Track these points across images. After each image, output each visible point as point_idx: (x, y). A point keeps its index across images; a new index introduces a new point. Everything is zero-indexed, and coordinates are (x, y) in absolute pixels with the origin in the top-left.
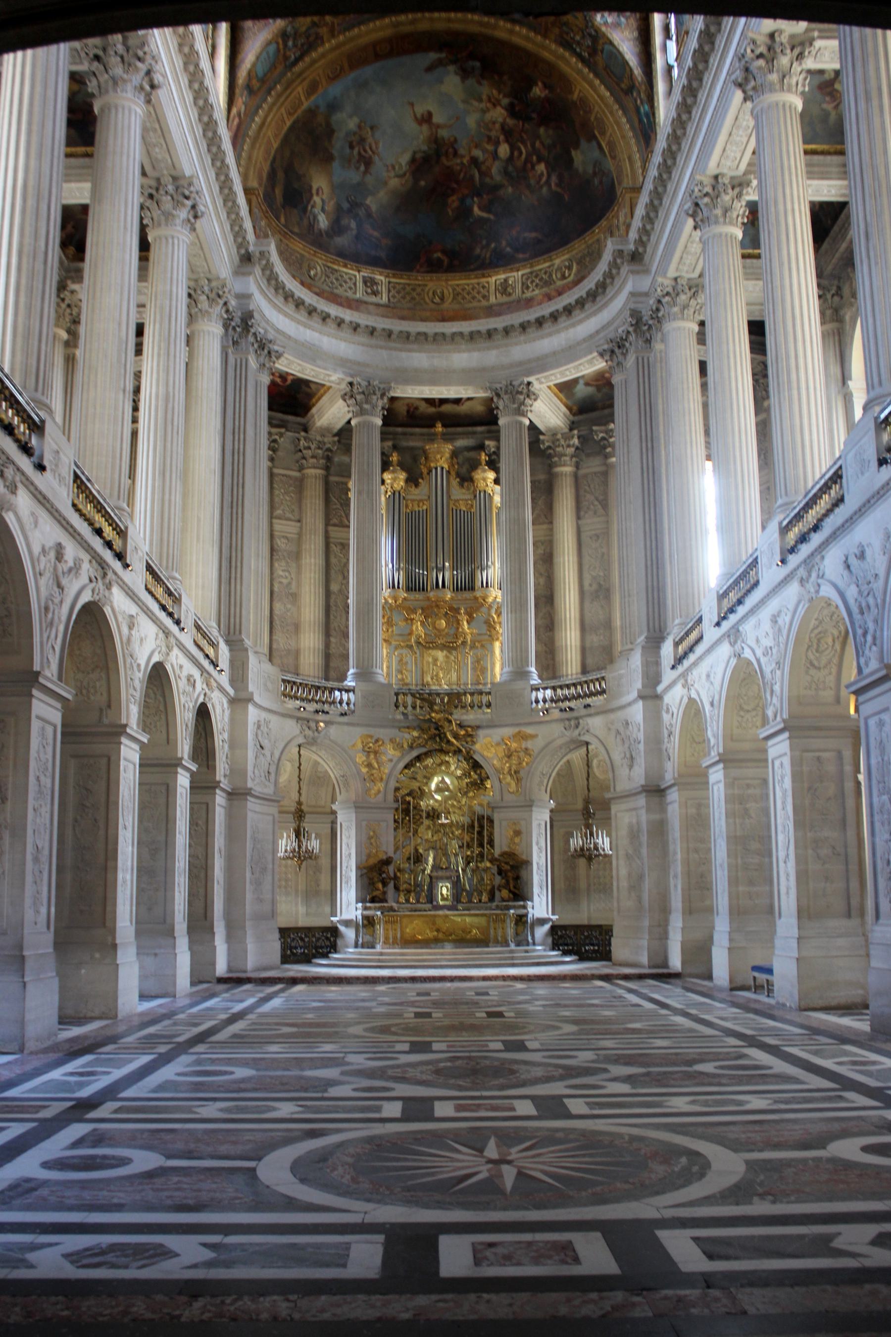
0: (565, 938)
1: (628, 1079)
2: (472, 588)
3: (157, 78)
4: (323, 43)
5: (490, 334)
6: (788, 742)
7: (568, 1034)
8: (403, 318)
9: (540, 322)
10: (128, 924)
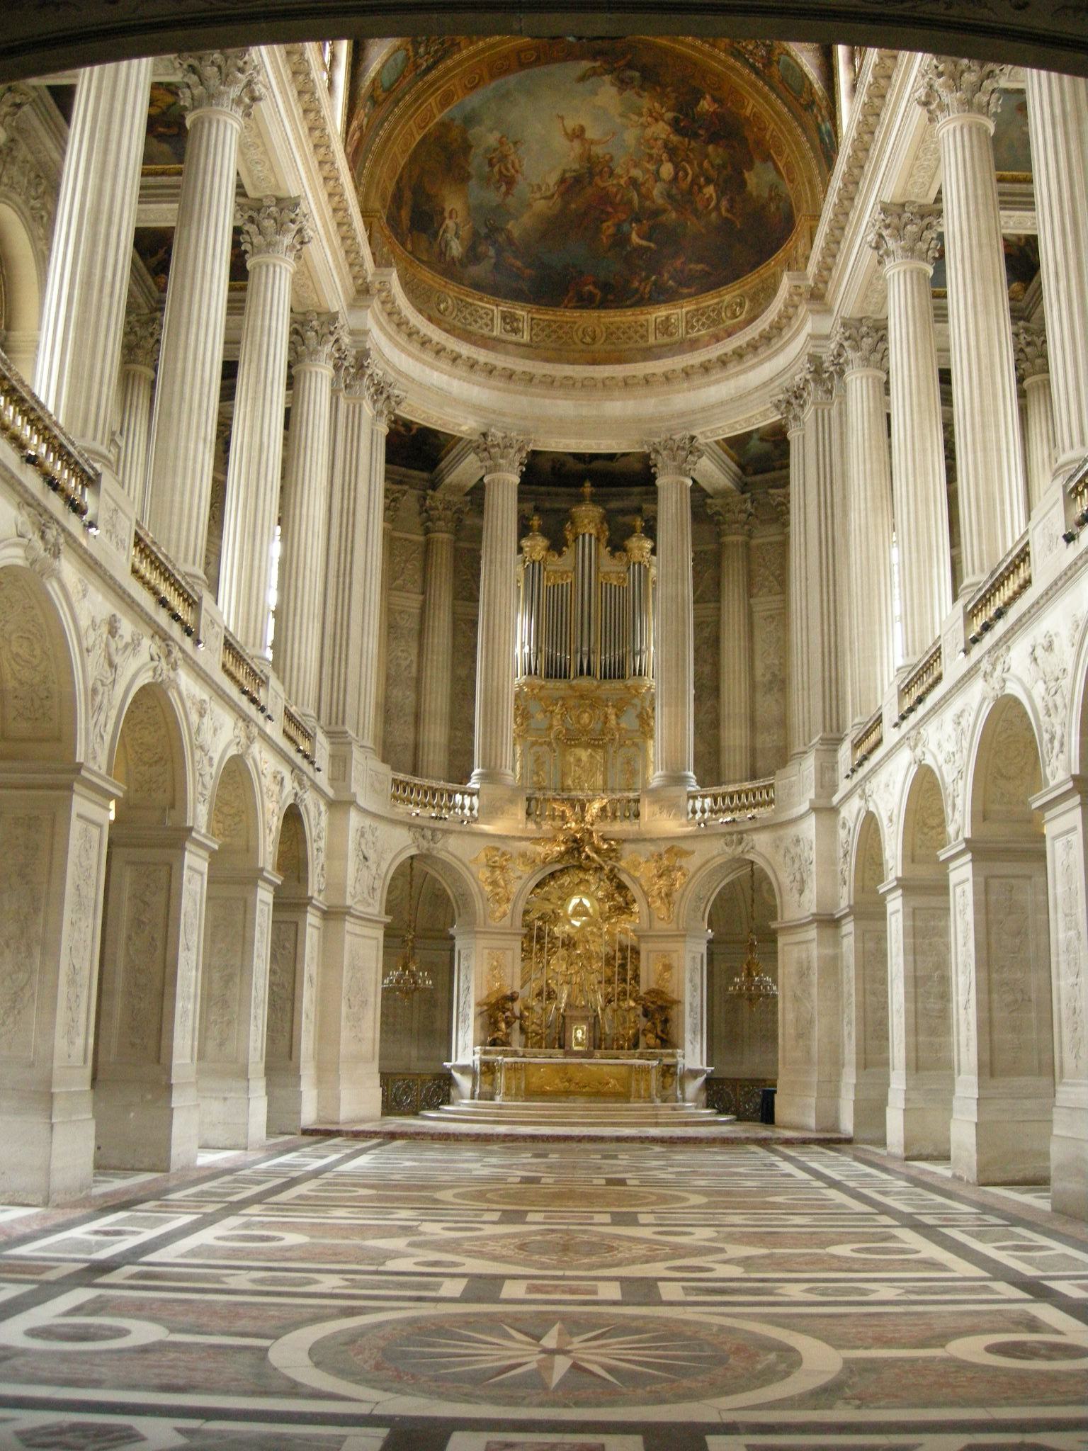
0: (719, 1093)
1: (746, 1262)
2: (623, 677)
3: (259, 89)
4: (460, 50)
5: (647, 381)
6: (970, 865)
7: (693, 1207)
8: (547, 360)
9: (706, 368)
10: (189, 1061)
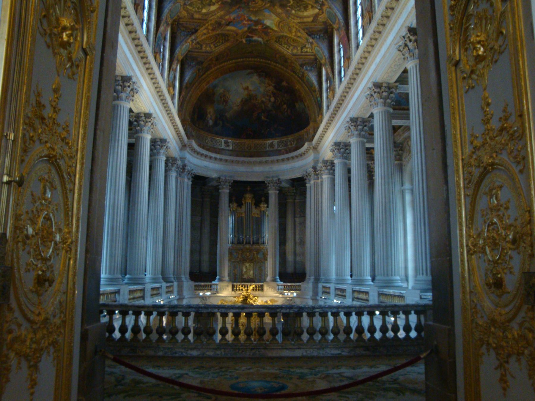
5: (266, 162)
8: (237, 156)
9: (283, 160)
